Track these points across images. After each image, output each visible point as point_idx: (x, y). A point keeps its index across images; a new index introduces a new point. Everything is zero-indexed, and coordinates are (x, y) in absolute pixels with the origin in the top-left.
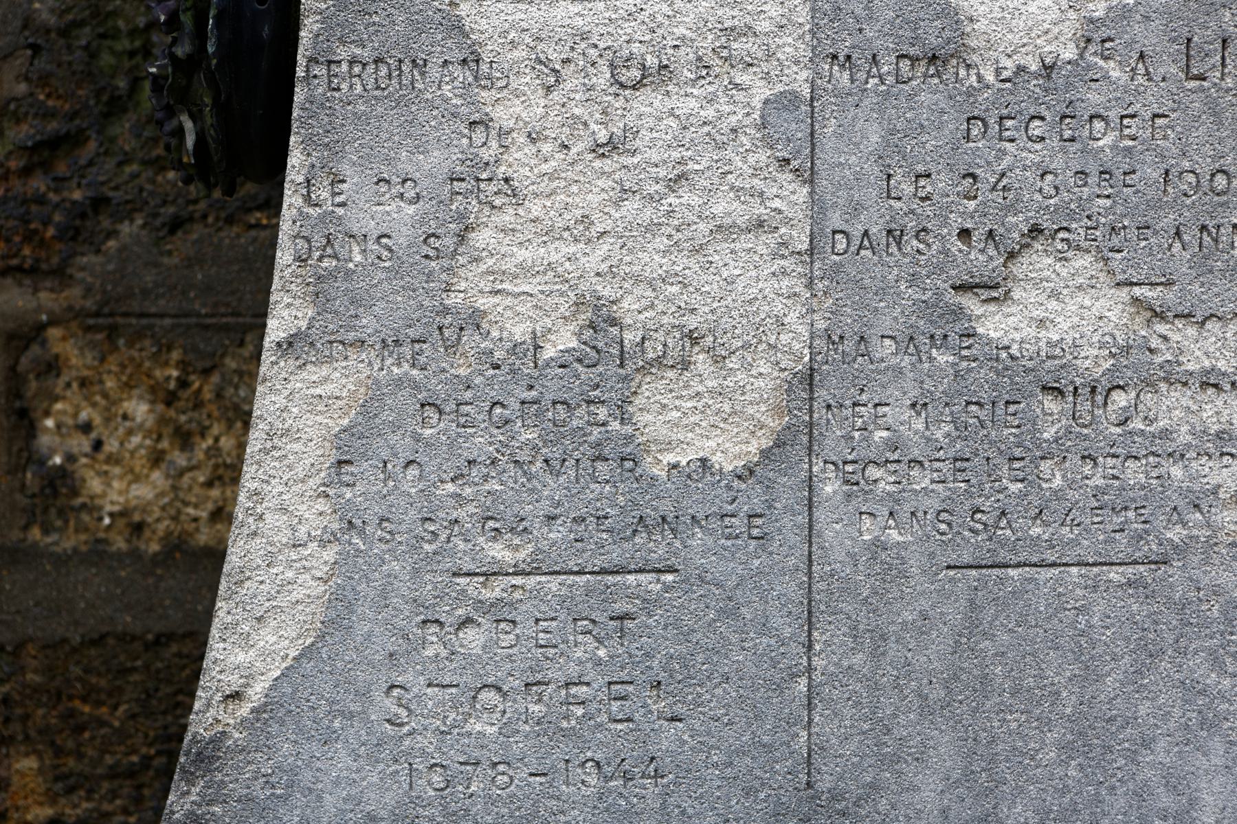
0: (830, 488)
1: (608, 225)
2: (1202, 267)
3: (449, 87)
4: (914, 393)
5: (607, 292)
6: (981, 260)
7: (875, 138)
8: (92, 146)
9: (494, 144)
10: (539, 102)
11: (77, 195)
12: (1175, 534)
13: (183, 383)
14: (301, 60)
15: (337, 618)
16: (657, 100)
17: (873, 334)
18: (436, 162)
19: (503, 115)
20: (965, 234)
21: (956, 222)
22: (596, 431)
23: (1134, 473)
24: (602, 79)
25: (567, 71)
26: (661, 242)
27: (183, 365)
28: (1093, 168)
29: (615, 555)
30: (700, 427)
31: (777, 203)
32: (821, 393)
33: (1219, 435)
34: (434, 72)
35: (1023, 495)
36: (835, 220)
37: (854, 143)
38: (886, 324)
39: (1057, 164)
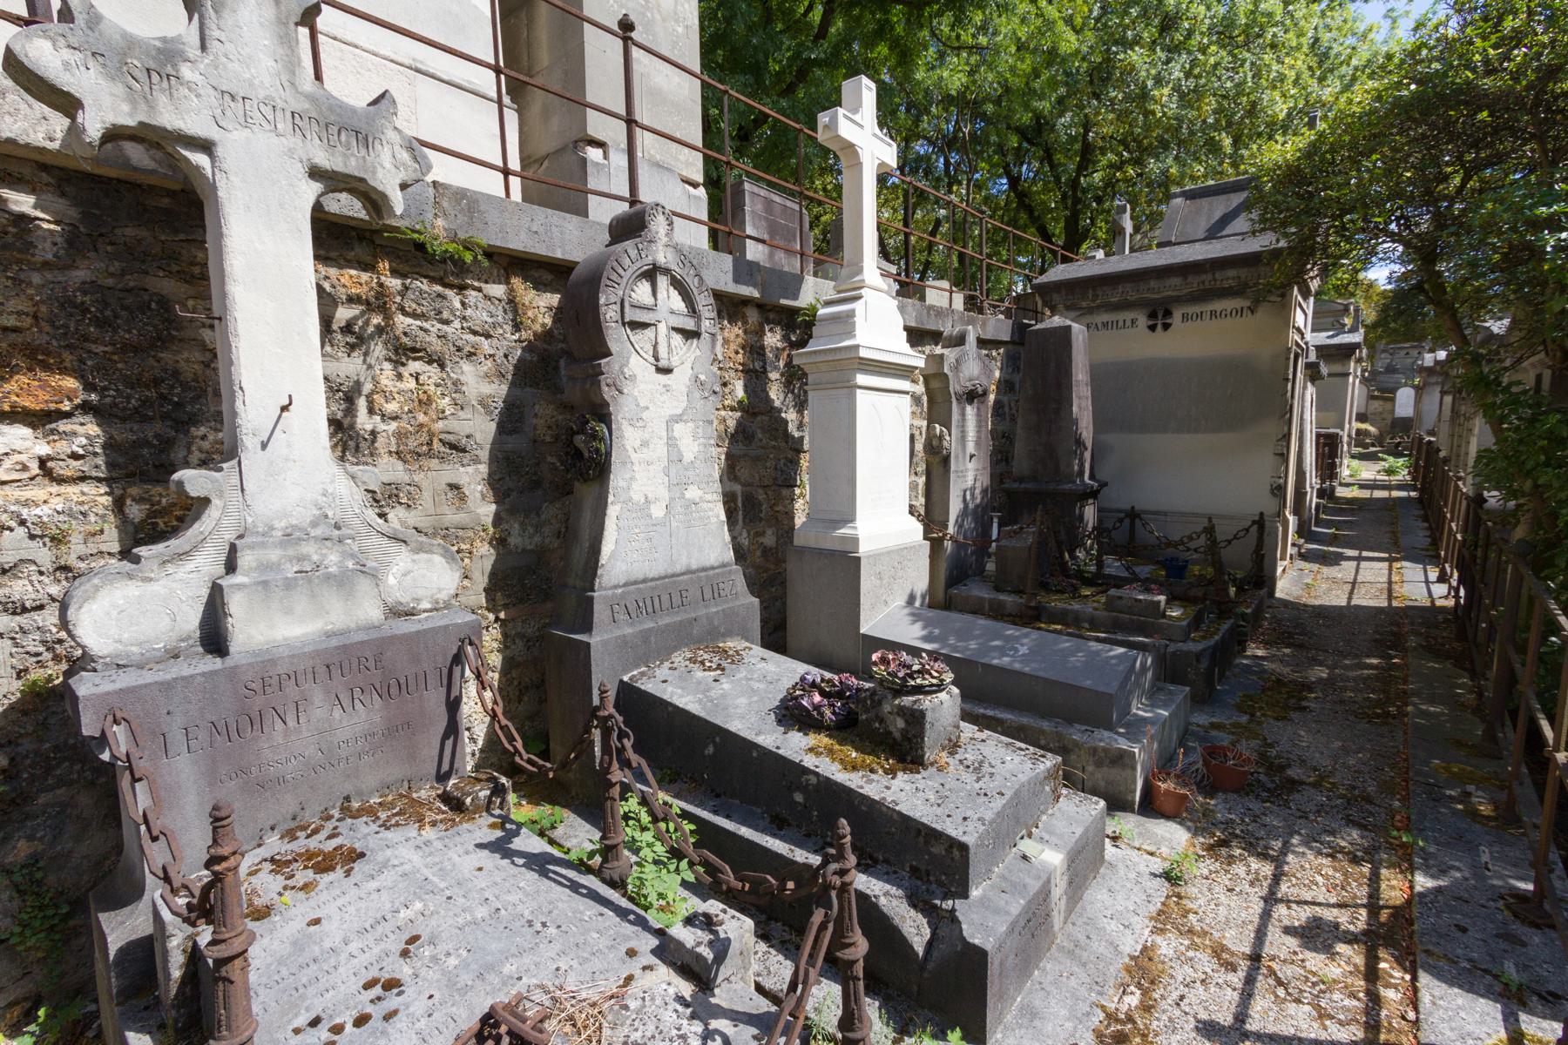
30: (658, 512)
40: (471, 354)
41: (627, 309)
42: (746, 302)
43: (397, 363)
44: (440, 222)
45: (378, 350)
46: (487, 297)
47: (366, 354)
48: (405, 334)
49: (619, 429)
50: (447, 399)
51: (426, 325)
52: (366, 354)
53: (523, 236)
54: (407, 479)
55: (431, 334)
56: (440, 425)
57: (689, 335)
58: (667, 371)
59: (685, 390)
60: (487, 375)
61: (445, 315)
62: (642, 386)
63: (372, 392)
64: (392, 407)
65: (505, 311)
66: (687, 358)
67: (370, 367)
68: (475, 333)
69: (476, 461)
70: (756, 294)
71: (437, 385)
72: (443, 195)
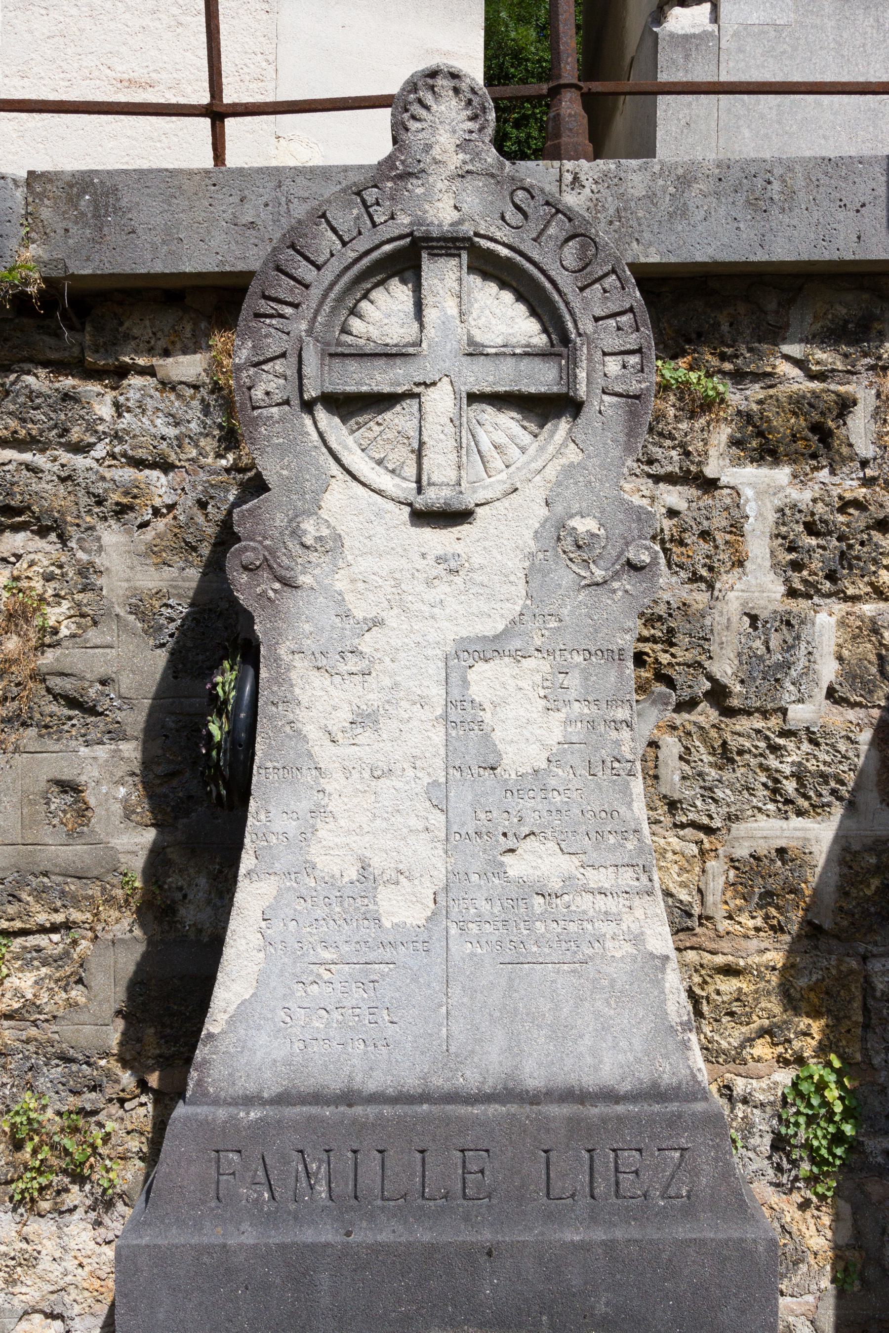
0: (454, 930)
1: (369, 829)
2: (596, 848)
3: (308, 777)
4: (486, 895)
5: (368, 854)
6: (511, 843)
7: (470, 797)
8: (187, 775)
10: (343, 781)
11: (180, 794)
12: (589, 951)
13: (220, 872)
14: (255, 767)
15: (261, 981)
16: (388, 782)
17: (470, 872)
18: (304, 806)
19: (329, 789)
20: (505, 835)
21: (501, 830)
22: (364, 908)
23: (573, 927)
24: (367, 775)
25: (353, 771)
26: (389, 836)
27: (220, 864)
28: (553, 809)
29: (371, 956)
31: (433, 822)
32: (450, 894)
33: (606, 913)
34: (304, 771)
35: (529, 935)
36: (455, 828)
37: (461, 799)
38: (474, 868)
39: (539, 807)
41: (311, 368)
44: (33, 251)
46: (168, 386)
49: (281, 679)
50: (66, 604)
53: (218, 240)
56: (49, 658)
57: (544, 408)
59: (516, 565)
60: (152, 550)
61: (76, 433)
62: (364, 565)
65: (206, 410)
66: (524, 477)
68: (139, 464)
69: (116, 734)
72: (42, 196)
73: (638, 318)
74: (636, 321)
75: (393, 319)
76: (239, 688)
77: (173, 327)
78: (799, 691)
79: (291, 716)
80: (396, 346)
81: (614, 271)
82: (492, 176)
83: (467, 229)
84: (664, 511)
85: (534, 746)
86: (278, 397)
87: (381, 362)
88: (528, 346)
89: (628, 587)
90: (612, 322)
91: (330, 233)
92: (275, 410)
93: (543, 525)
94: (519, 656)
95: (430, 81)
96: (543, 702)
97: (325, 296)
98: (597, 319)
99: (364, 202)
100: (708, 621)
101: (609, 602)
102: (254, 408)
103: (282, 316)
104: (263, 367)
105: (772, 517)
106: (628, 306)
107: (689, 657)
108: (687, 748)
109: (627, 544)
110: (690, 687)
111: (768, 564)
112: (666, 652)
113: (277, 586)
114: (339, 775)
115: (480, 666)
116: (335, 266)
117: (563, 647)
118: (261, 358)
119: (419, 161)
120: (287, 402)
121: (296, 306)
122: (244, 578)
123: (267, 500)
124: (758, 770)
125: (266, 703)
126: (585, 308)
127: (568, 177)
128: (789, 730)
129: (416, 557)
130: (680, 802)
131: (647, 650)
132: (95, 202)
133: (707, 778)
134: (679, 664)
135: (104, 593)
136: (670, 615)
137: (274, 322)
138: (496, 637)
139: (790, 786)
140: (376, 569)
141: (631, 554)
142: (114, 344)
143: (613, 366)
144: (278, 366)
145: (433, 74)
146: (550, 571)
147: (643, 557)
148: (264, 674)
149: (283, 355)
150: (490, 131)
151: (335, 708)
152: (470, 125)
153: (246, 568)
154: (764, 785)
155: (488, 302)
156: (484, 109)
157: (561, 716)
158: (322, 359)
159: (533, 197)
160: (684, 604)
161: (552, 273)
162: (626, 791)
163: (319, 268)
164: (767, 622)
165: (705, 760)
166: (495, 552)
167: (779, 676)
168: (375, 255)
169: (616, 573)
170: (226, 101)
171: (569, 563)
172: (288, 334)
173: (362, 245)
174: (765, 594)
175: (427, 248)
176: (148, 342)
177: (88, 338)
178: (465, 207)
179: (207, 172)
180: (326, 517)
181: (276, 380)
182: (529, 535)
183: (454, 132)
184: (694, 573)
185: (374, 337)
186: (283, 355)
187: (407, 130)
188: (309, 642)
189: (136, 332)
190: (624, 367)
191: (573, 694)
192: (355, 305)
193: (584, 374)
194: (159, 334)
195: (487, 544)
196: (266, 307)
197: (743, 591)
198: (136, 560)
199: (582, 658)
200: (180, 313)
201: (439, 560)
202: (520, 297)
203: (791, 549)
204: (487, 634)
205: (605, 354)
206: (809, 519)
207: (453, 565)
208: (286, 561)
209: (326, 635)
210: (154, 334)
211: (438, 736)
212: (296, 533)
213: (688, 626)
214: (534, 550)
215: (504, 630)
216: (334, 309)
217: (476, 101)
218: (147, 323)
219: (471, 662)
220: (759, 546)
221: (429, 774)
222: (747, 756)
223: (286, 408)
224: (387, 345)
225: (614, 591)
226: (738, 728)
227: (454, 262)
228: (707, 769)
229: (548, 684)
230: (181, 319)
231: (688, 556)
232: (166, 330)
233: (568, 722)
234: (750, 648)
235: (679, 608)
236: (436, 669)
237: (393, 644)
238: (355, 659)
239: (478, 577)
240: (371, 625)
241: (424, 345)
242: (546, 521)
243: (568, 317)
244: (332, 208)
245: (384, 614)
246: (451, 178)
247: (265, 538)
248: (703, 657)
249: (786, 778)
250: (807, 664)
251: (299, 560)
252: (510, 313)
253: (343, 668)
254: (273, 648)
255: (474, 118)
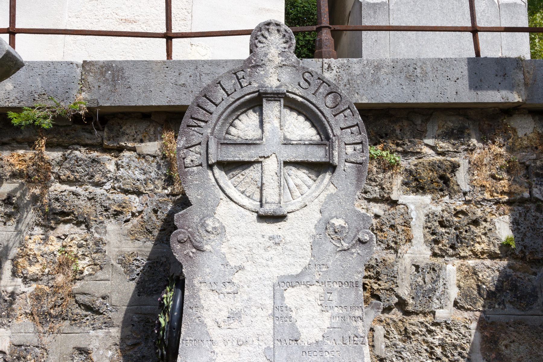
7: (285, 355)
8: (143, 345)
9: (215, 356)
10: (223, 347)
11: (139, 355)
14: (181, 340)
16: (245, 347)
19: (216, 351)
24: (235, 343)
25: (228, 342)
34: (205, 342)
40: (117, 214)
42: (508, 111)
43: (48, 228)
44: (83, 95)
45: (30, 216)
46: (141, 156)
47: (18, 222)
48: (57, 200)
49: (195, 296)
50: (87, 259)
51: (80, 190)
52: (18, 222)
53: (168, 91)
54: (35, 341)
55: (79, 196)
56: (77, 286)
57: (318, 168)
58: (277, 218)
59: (306, 241)
60: (131, 233)
61: (97, 178)
63: (19, 256)
64: (34, 270)
65: (159, 167)
66: (310, 199)
67: (20, 232)
68: (126, 192)
69: (108, 324)
70: (515, 98)
71: (80, 246)
73: (360, 129)
74: (359, 130)
75: (250, 128)
76: (174, 300)
77: (145, 129)
78: (441, 303)
79: (199, 314)
80: (251, 140)
81: (349, 108)
82: (295, 67)
83: (283, 89)
84: (373, 215)
85: (316, 329)
86: (196, 163)
87: (244, 147)
88: (311, 140)
89: (359, 252)
90: (349, 130)
91: (222, 91)
92: (195, 168)
93: (319, 222)
94: (308, 285)
95: (267, 27)
96: (320, 307)
97: (219, 118)
98: (342, 129)
99: (237, 77)
100: (395, 268)
101: (351, 258)
102: (185, 167)
103: (199, 126)
104: (190, 149)
105: (423, 218)
106: (356, 123)
107: (387, 286)
108: (388, 332)
109: (358, 231)
110: (388, 300)
111: (423, 241)
112: (376, 283)
113: (194, 250)
114: (221, 344)
115: (290, 290)
116: (224, 105)
117: (329, 280)
118: (190, 145)
119: (262, 60)
120: (201, 165)
121: (206, 122)
122: (179, 246)
123: (190, 210)
124: (422, 343)
125: (187, 308)
126: (337, 124)
127: (326, 66)
128: (437, 322)
129: (260, 237)
130: (385, 359)
131: (367, 282)
132: (113, 75)
133: (398, 347)
134: (382, 289)
135: (106, 253)
136: (377, 265)
137: (196, 129)
138: (298, 275)
139: (438, 351)
140: (241, 242)
141: (360, 236)
142: (118, 137)
143: (350, 150)
144: (197, 148)
145: (269, 24)
146: (323, 244)
147: (366, 238)
148: (186, 293)
149: (200, 144)
150: (293, 48)
151: (220, 310)
152: (285, 45)
153: (179, 242)
154: (426, 350)
155: (293, 121)
156: (291, 39)
157: (329, 314)
158: (218, 146)
159: (312, 76)
160: (384, 260)
161: (322, 109)
162: (361, 352)
163: (217, 105)
164: (423, 269)
165: (397, 338)
166: (297, 235)
167: (430, 295)
168: (242, 100)
169: (354, 245)
170: (173, 31)
171: (331, 240)
172: (202, 134)
173: (236, 96)
174: (422, 255)
175: (265, 97)
176: (133, 136)
177: (105, 134)
178: (282, 80)
179: (164, 62)
180: (218, 218)
181: (196, 155)
182: (312, 227)
183: (278, 48)
184: (388, 245)
185: (241, 136)
186: (200, 144)
187: (257, 47)
188: (208, 277)
189: (128, 131)
190: (355, 150)
191: (334, 303)
192: (233, 122)
193: (337, 153)
194: (138, 133)
195: (293, 231)
196: (192, 122)
197: (411, 254)
198: (122, 238)
199: (338, 286)
200: (149, 123)
201: (271, 238)
202: (307, 119)
203: (433, 234)
204: (293, 274)
205: (346, 144)
206: (441, 219)
207: (277, 240)
208: (198, 239)
209: (216, 274)
210: (136, 132)
211: (270, 324)
212: (203, 225)
213: (386, 271)
214: (315, 234)
215: (301, 272)
216: (223, 124)
217: (287, 35)
218: (133, 127)
219: (285, 287)
220: (418, 232)
221: (265, 343)
222: (417, 336)
223: (200, 167)
224: (247, 139)
225: (353, 254)
226: (412, 321)
227: (277, 103)
228: (398, 342)
229: (322, 298)
230: (149, 126)
231: (385, 237)
232: (142, 131)
233: (332, 317)
234: (416, 281)
235: (381, 262)
236: (269, 291)
237: (249, 278)
238: (230, 286)
239: (288, 247)
240: (238, 269)
241: (264, 140)
242: (320, 220)
243: (329, 128)
244: (223, 80)
245: (244, 264)
246: (276, 68)
247: (189, 228)
248: (394, 286)
249: (436, 346)
250: (444, 289)
251: (205, 238)
252: (303, 126)
253: (224, 290)
254: (191, 280)
255: (286, 42)
